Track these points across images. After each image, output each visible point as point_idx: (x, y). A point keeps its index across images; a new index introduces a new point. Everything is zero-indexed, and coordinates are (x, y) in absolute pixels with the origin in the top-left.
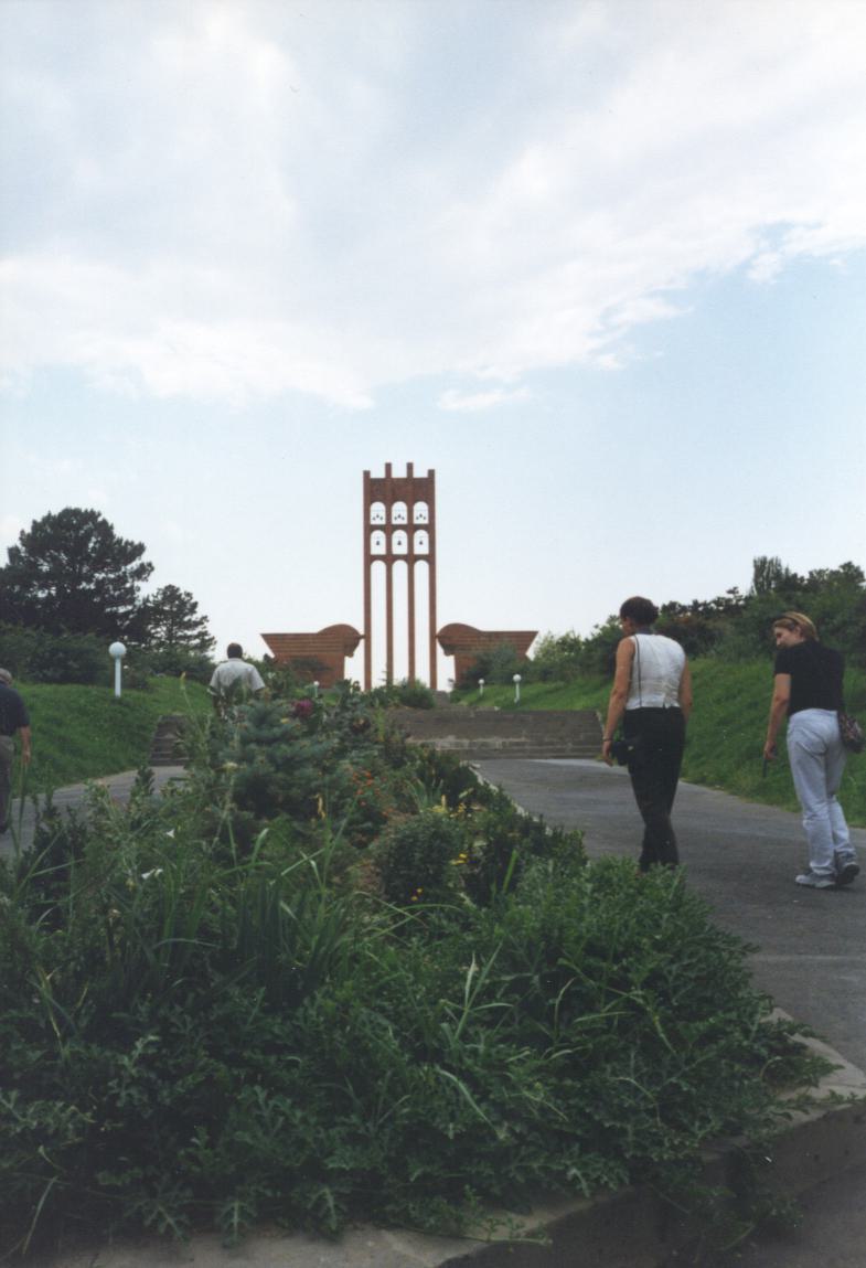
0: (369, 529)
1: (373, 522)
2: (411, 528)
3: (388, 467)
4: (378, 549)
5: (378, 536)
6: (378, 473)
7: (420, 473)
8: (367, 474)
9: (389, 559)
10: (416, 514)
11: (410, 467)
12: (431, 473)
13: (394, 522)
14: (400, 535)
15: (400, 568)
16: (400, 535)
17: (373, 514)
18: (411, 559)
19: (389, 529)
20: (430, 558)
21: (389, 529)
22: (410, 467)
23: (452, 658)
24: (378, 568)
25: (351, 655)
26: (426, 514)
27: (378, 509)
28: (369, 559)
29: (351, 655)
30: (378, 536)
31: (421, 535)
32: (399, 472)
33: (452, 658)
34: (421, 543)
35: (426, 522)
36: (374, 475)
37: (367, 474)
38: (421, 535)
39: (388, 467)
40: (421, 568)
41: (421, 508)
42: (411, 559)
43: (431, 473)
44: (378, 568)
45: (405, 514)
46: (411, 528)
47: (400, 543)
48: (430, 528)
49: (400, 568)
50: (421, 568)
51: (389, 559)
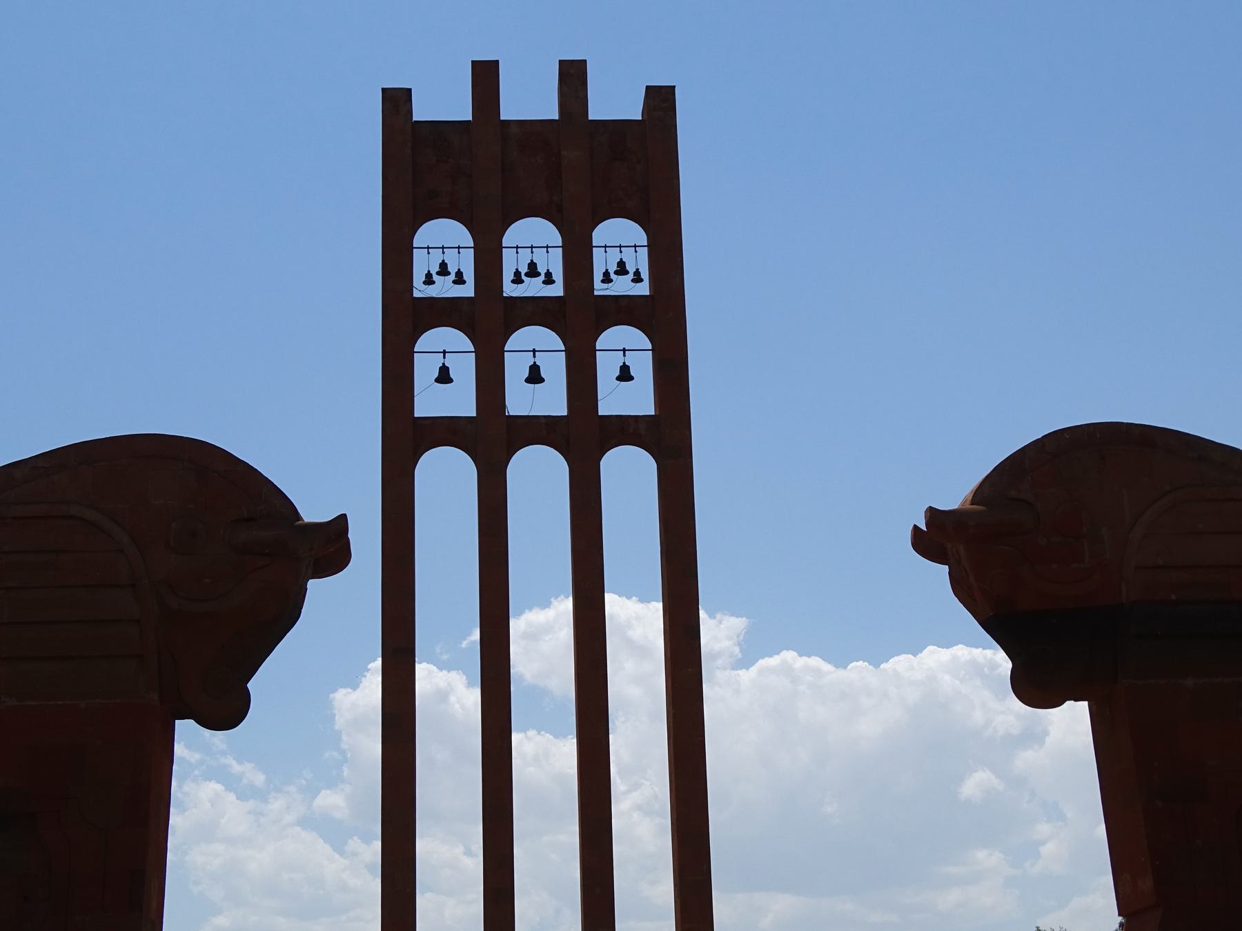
0: (405, 317)
1: (420, 290)
2: (579, 317)
3: (485, 77)
4: (446, 397)
5: (444, 345)
6: (444, 101)
7: (614, 100)
8: (396, 102)
9: (491, 439)
10: (602, 262)
11: (573, 77)
12: (661, 101)
13: (510, 290)
14: (534, 344)
15: (539, 476)
16: (534, 344)
17: (422, 264)
18: (583, 437)
19: (489, 319)
20: (667, 435)
21: (489, 319)
22: (573, 77)
23: (1072, 721)
24: (445, 477)
25: (226, 710)
26: (640, 261)
27: (443, 243)
28: (406, 438)
29: (226, 710)
30: (444, 345)
31: (622, 345)
32: (529, 99)
33: (1072, 721)
34: (625, 375)
35: (643, 289)
36: (421, 112)
37: (396, 102)
38: (622, 345)
39: (485, 77)
40: (629, 475)
41: (619, 241)
42: (583, 437)
43: (661, 101)
44: (445, 477)
45: (554, 262)
46: (579, 317)
47: (535, 376)
48: (662, 316)
49: (539, 476)
50: (629, 475)
51: (491, 439)
